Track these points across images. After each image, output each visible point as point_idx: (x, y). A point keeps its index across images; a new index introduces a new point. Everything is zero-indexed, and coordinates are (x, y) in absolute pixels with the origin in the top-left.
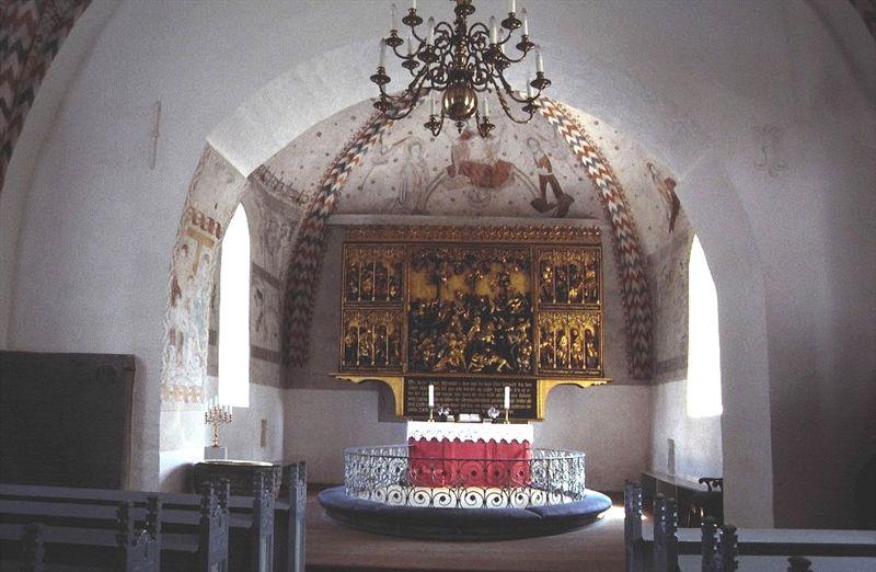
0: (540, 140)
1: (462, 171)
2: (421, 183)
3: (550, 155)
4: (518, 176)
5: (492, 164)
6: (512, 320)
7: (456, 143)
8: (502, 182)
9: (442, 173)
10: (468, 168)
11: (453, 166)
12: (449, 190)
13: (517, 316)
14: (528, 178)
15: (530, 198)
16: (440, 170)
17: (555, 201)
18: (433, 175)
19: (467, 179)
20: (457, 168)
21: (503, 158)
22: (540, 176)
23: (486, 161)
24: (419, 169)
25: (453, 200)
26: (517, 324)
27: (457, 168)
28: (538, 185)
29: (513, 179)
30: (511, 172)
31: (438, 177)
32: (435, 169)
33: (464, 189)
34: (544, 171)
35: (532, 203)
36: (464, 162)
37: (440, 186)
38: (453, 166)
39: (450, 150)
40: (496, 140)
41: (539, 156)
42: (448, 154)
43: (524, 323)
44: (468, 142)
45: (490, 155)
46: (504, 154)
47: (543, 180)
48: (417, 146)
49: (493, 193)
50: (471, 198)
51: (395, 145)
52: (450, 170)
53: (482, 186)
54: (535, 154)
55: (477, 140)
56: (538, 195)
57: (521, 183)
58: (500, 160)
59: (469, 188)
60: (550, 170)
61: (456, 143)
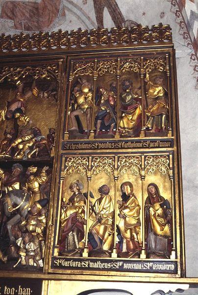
4: (69, 10)
6: (17, 170)
13: (26, 164)
14: (81, 9)
26: (24, 179)
29: (64, 15)
30: (61, 7)
43: (37, 175)
57: (74, 18)
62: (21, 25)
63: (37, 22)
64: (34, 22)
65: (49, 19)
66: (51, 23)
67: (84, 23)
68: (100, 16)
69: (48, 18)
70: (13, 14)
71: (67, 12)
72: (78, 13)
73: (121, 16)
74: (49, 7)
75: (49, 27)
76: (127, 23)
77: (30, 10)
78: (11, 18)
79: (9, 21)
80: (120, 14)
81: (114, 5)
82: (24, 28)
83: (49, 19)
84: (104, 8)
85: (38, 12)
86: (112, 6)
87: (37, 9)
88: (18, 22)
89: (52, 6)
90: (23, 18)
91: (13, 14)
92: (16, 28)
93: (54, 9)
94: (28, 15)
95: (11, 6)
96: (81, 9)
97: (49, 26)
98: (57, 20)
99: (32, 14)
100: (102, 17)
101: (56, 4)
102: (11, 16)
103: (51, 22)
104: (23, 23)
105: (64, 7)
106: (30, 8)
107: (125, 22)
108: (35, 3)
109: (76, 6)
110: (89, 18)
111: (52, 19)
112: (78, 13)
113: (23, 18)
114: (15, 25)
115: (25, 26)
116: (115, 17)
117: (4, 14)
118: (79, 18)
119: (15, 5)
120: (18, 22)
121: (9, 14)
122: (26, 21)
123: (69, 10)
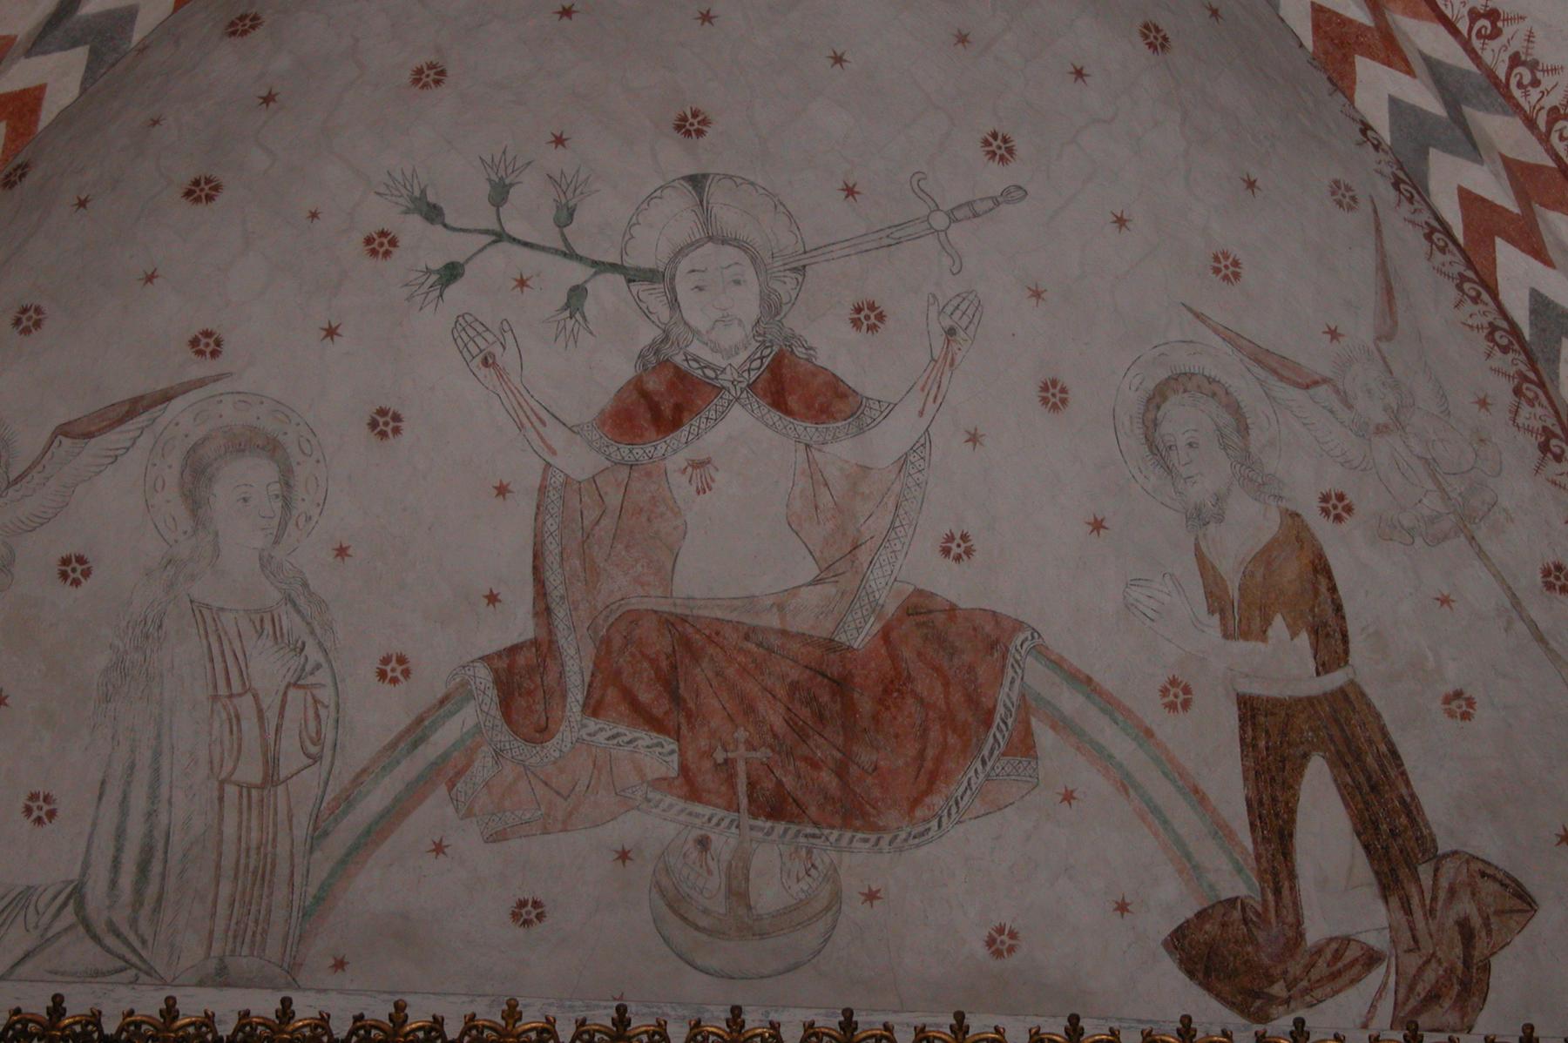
0: (1244, 384)
1: (611, 691)
2: (271, 778)
3: (1336, 506)
4: (1062, 724)
5: (860, 635)
7: (580, 459)
8: (932, 778)
9: (446, 703)
10: (664, 670)
11: (544, 648)
12: (498, 837)
15: (1171, 902)
16: (430, 680)
17: (1371, 921)
18: (378, 714)
19: (655, 755)
20: (576, 664)
21: (952, 585)
22: (1249, 709)
23: (810, 613)
24: (267, 668)
25: (528, 913)
27: (576, 664)
28: (1228, 787)
29: (1024, 745)
30: (1005, 697)
31: (417, 732)
32: (393, 669)
33: (626, 829)
34: (1284, 664)
35: (1179, 942)
36: (634, 617)
37: (434, 812)
38: (544, 648)
39: (523, 506)
40: (889, 439)
41: (1245, 531)
42: (502, 546)
44: (673, 454)
45: (842, 560)
46: (956, 547)
47: (1273, 740)
48: (257, 474)
49: (855, 859)
50: (675, 902)
51: (75, 431)
52: (520, 683)
53: (776, 806)
54: (1198, 518)
55: (738, 432)
56: (1233, 879)
58: (918, 608)
59: (663, 824)
60: (1331, 641)
61: (580, 459)
62: (731, 779)
63: (841, 772)
64: (815, 765)
65: (922, 752)
66: (929, 791)
67: (1165, 822)
68: (1274, 800)
69: (911, 750)
70: (676, 699)
71: (1044, 736)
72: (1121, 746)
73: (1413, 821)
74: (925, 684)
75: (919, 813)
76: (1449, 868)
77: (794, 687)
78: (656, 724)
79: (646, 738)
80: (1411, 808)
81: (1379, 757)
82: (750, 796)
83: (922, 752)
84: (1306, 756)
85: (849, 708)
86: (1359, 757)
87: (841, 685)
88: (709, 754)
89: (946, 685)
90: (741, 734)
91: (676, 699)
92: (694, 793)
93: (957, 697)
94: (775, 717)
95: (660, 644)
96: (1149, 733)
97: (916, 802)
98: (974, 773)
99: (805, 713)
100: (1292, 812)
101: (971, 669)
102: (659, 711)
103: (933, 778)
104: (741, 768)
105: (1025, 707)
106: (795, 674)
107: (1438, 860)
108: (830, 645)
109: (1110, 705)
110: (1198, 797)
111: (938, 760)
112: (1121, 746)
113: (741, 734)
114: (684, 769)
115: (752, 785)
116: (1375, 825)
117: (612, 694)
118: (1126, 784)
119: (687, 643)
120: (709, 754)
121: (645, 697)
122: (762, 754)
123: (1062, 724)
